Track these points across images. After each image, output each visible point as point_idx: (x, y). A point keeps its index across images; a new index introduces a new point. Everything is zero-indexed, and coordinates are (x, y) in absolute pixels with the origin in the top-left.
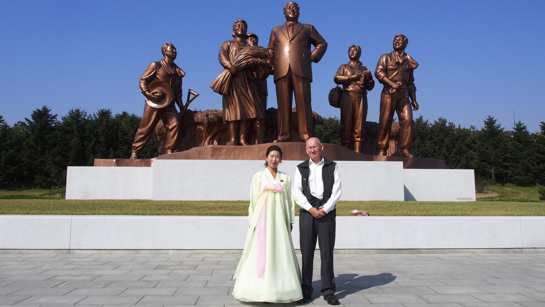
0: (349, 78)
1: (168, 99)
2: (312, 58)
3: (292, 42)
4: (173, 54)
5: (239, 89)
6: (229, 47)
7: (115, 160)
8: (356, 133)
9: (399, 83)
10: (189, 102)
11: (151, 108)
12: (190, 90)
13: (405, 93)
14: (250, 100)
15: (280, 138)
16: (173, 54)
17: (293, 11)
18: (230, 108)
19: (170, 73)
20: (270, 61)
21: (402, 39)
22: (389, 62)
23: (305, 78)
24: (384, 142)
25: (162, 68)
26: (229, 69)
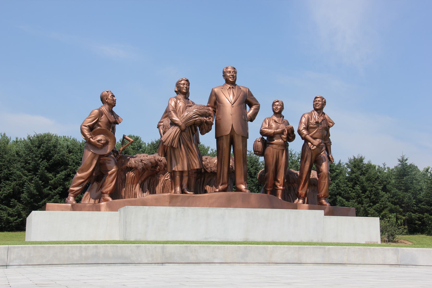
3: (234, 105)
8: (278, 182)
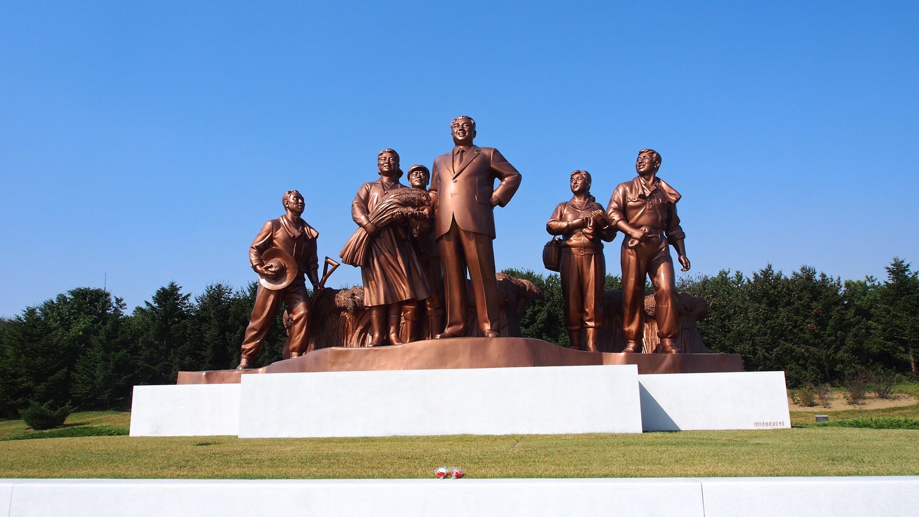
0: (568, 225)
1: (288, 275)
2: (494, 200)
3: (457, 179)
4: (298, 206)
5: (383, 256)
6: (368, 193)
7: (204, 373)
8: (587, 314)
9: (644, 229)
10: (326, 275)
11: (265, 290)
12: (327, 258)
13: (661, 243)
14: (400, 272)
15: (447, 331)
16: (298, 206)
17: (463, 130)
18: (370, 286)
19: (293, 236)
20: (429, 209)
21: (648, 157)
22: (630, 196)
23: (480, 234)
24: (633, 327)
25: (281, 229)
26: (364, 227)
